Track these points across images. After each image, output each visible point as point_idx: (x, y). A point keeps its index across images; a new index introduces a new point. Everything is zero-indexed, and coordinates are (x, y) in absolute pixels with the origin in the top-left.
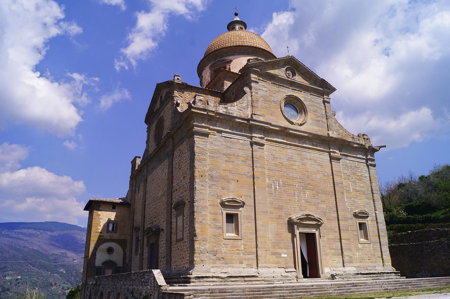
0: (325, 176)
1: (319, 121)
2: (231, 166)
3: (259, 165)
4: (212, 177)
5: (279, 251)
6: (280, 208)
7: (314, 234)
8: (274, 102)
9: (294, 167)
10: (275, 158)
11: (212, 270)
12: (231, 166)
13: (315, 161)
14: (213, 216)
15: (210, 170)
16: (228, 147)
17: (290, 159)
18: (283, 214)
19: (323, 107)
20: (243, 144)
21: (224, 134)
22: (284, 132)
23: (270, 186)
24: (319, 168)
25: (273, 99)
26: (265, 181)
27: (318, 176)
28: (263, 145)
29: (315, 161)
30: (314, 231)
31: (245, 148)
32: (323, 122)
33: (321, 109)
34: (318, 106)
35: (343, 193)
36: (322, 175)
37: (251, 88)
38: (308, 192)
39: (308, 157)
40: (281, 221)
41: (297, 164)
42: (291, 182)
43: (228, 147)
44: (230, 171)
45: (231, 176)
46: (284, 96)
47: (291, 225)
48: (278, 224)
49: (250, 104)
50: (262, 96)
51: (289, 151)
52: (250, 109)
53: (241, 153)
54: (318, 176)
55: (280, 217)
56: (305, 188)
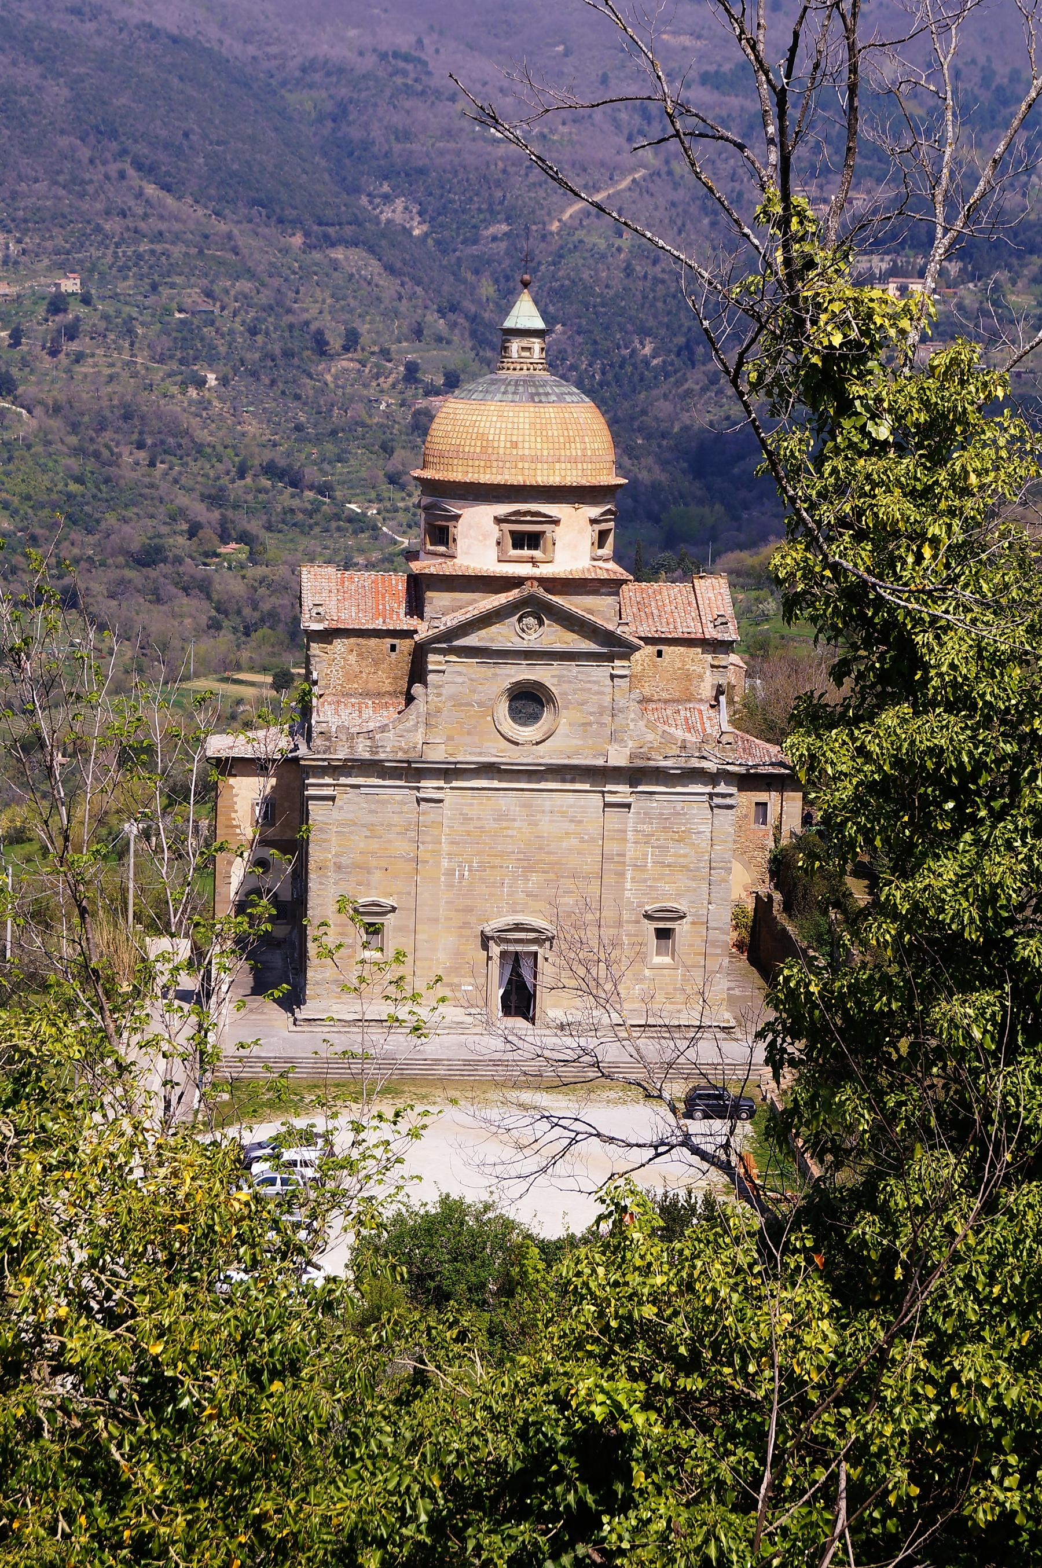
0: (582, 841)
1: (590, 724)
2: (374, 845)
3: (428, 839)
4: (339, 867)
5: (456, 980)
6: (468, 910)
7: (536, 954)
8: (480, 704)
9: (510, 832)
10: (467, 819)
11: (335, 1007)
12: (374, 845)
13: (563, 814)
14: (339, 929)
15: (337, 855)
16: (370, 812)
17: (501, 817)
18: (473, 920)
19: (609, 690)
20: (403, 803)
21: (363, 790)
22: (489, 770)
23: (450, 873)
24: (573, 826)
25: (476, 697)
26: (438, 865)
27: (565, 845)
28: (441, 801)
29: (563, 814)
30: (534, 948)
31: (405, 808)
32: (602, 725)
33: (603, 693)
34: (596, 688)
35: (622, 874)
36: (574, 842)
37: (425, 684)
38: (534, 877)
39: (547, 809)
40: (467, 932)
41: (516, 824)
42: (497, 861)
43: (370, 812)
44: (373, 854)
45: (374, 863)
46: (507, 684)
47: (485, 941)
48: (461, 936)
49: (422, 719)
50: (451, 697)
51: (502, 801)
52: (422, 730)
53: (396, 818)
54: (565, 845)
55: (466, 925)
56: (529, 869)
